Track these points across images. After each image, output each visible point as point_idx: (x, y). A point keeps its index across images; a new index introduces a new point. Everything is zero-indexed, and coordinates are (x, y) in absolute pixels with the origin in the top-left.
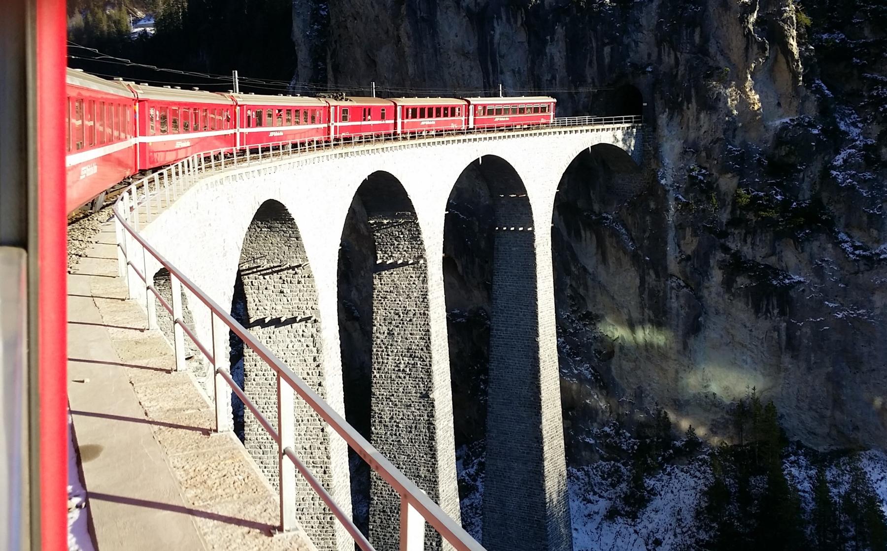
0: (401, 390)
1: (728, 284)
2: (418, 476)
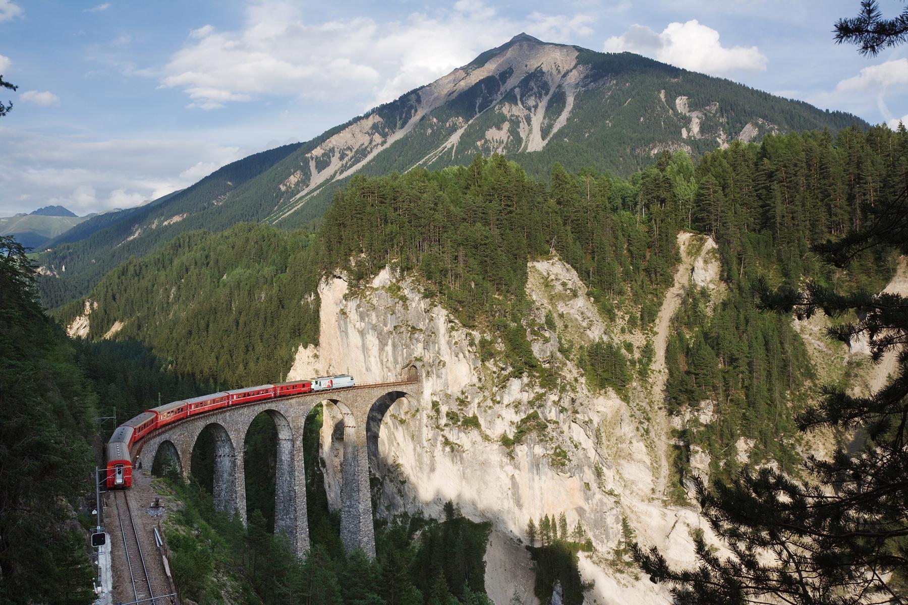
1: (443, 451)
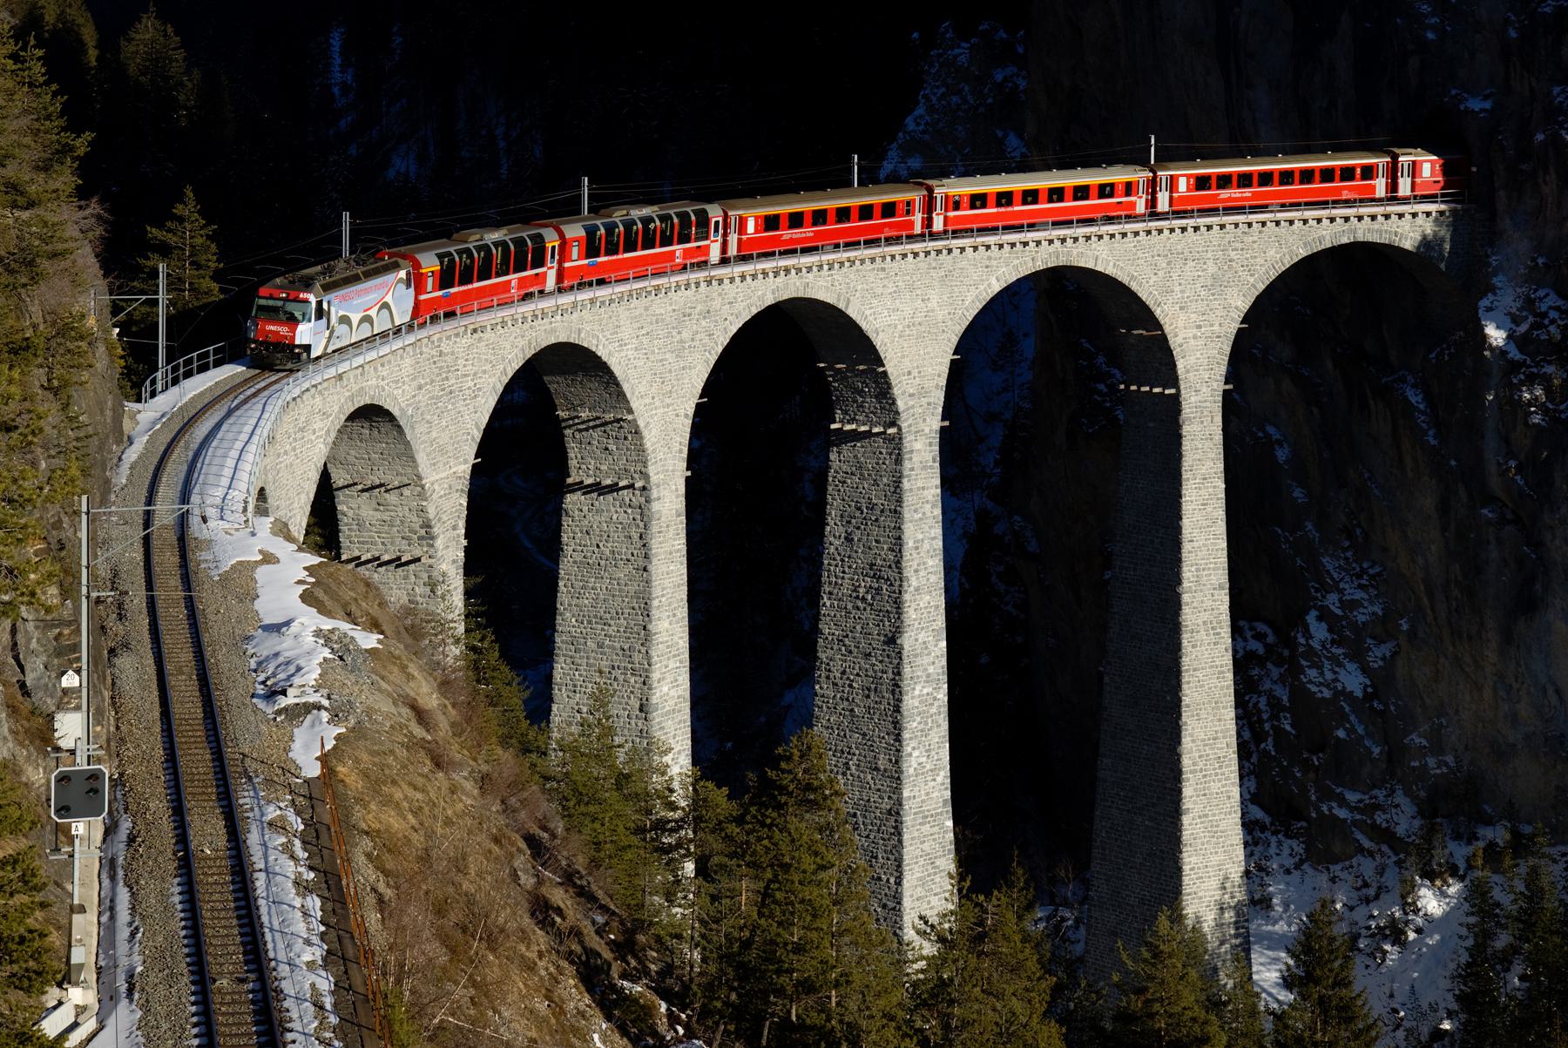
0: (858, 628)
2: (877, 769)
